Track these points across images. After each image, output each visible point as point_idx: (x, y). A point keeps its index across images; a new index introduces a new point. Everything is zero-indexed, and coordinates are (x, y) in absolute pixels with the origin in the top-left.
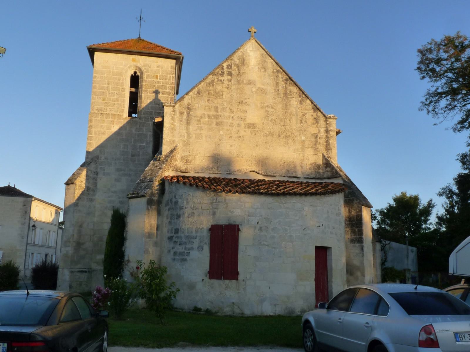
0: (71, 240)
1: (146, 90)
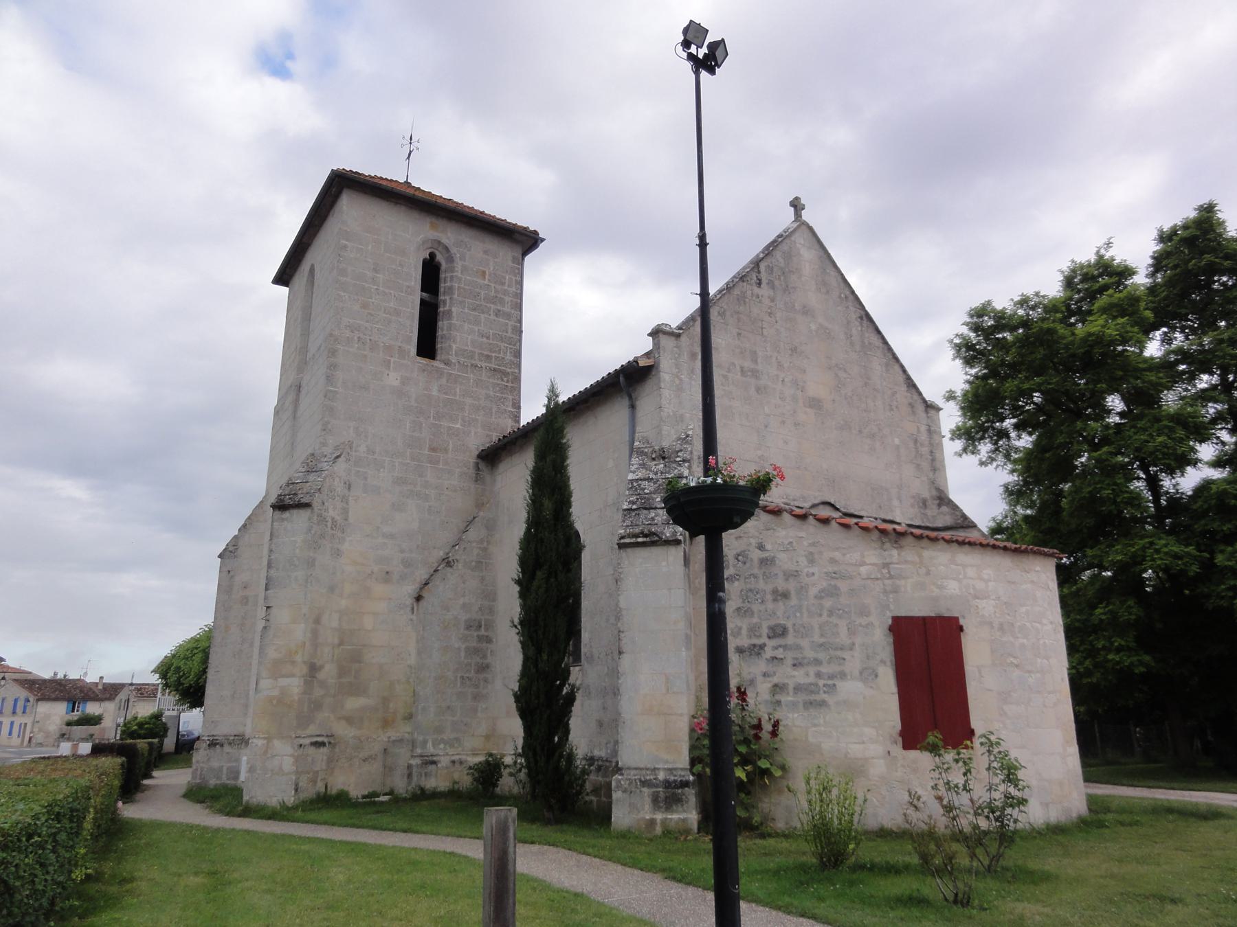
0: (299, 658)
1: (460, 299)
